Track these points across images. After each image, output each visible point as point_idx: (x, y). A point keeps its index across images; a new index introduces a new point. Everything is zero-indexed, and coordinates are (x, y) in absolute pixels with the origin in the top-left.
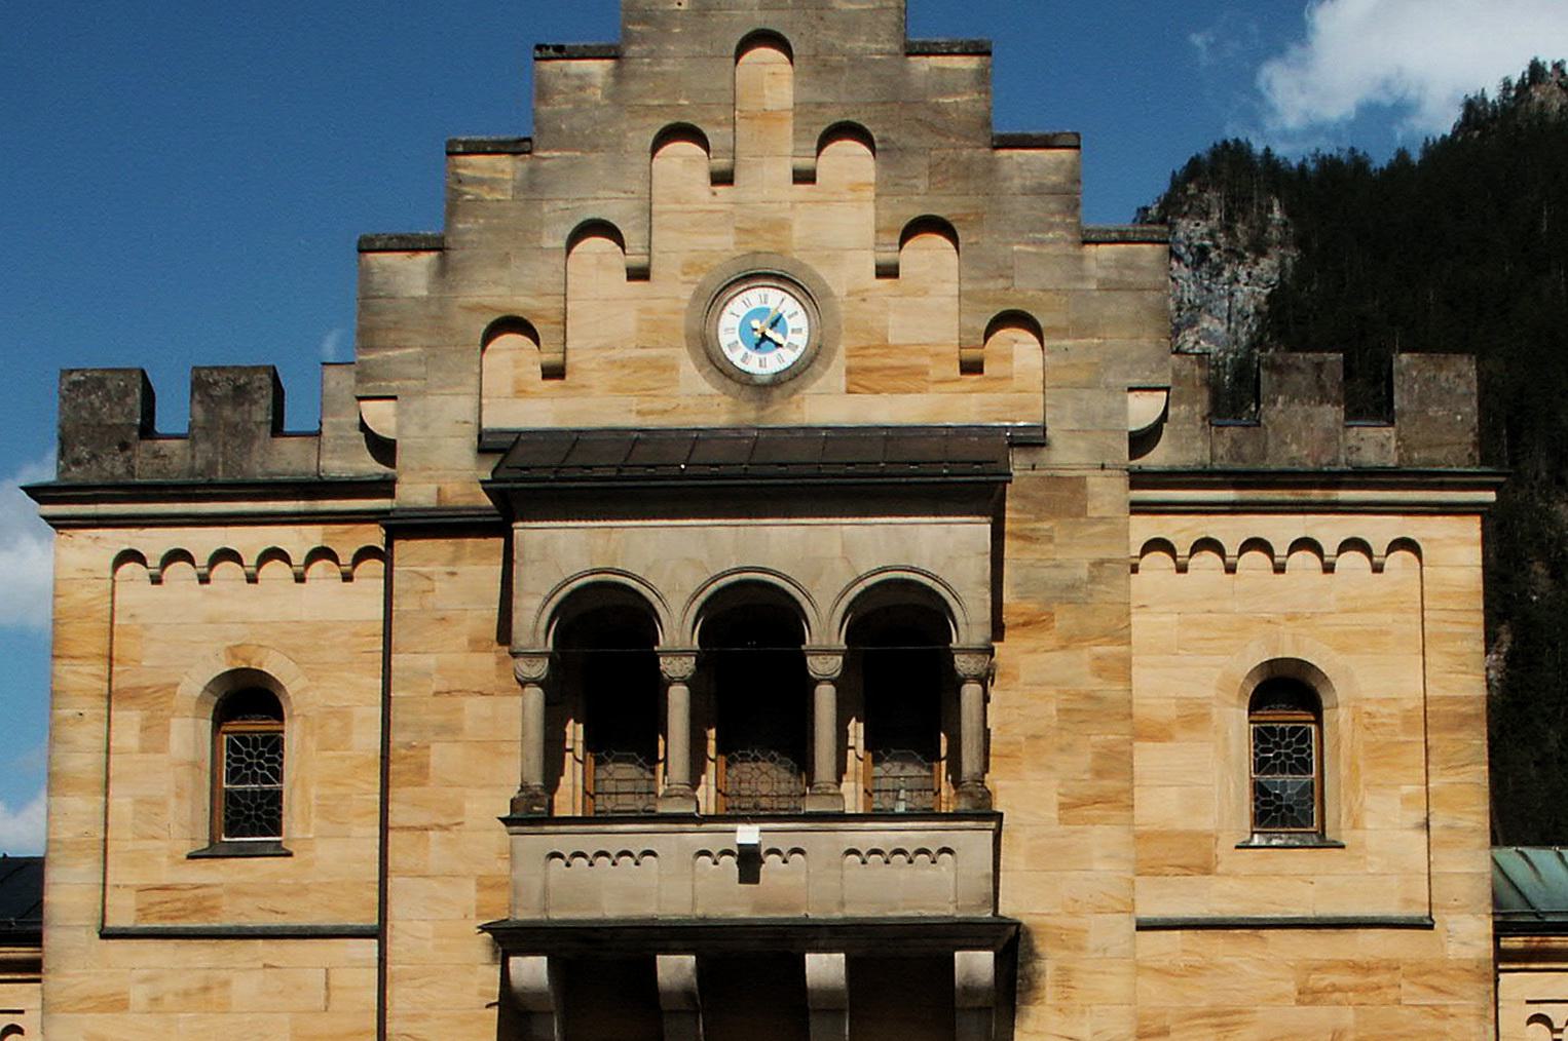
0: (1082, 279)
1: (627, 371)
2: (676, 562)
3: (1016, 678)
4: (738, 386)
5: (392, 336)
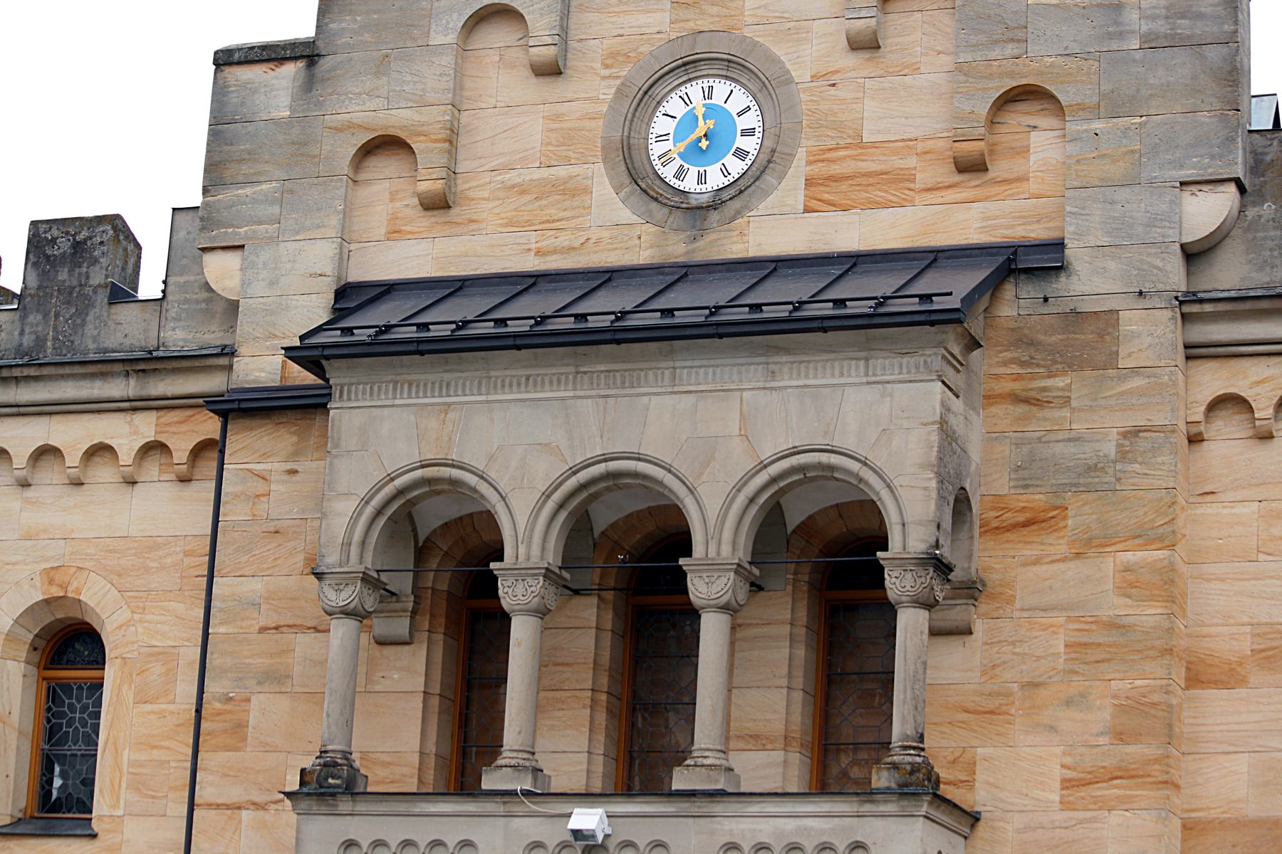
1: (528, 198)
2: (523, 448)
3: (1011, 600)
4: (666, 210)
5: (245, 169)
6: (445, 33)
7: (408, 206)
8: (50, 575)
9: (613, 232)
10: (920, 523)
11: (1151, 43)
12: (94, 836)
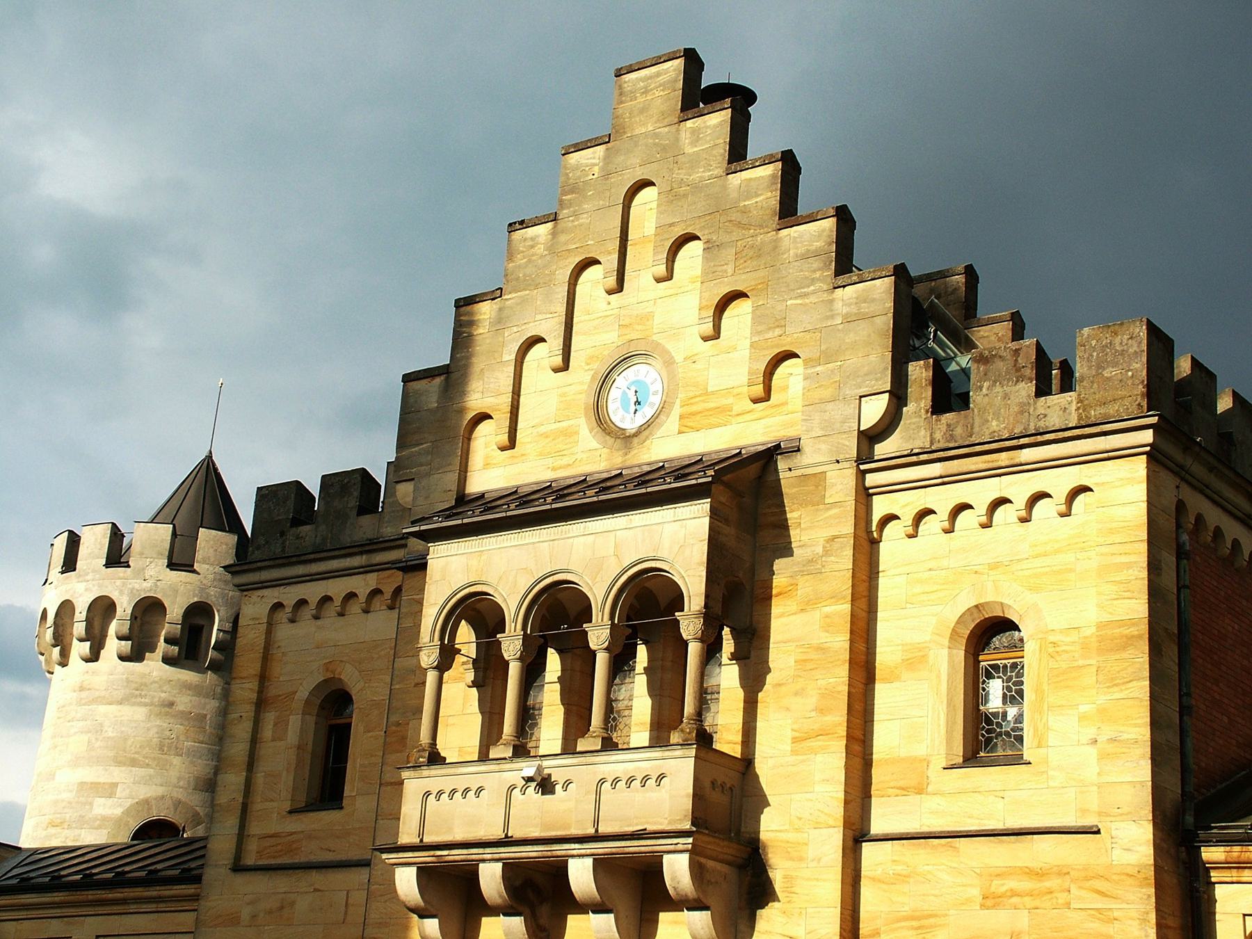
0: (832, 317)
6: (510, 356)
8: (327, 667)
10: (696, 595)
11: (848, 320)
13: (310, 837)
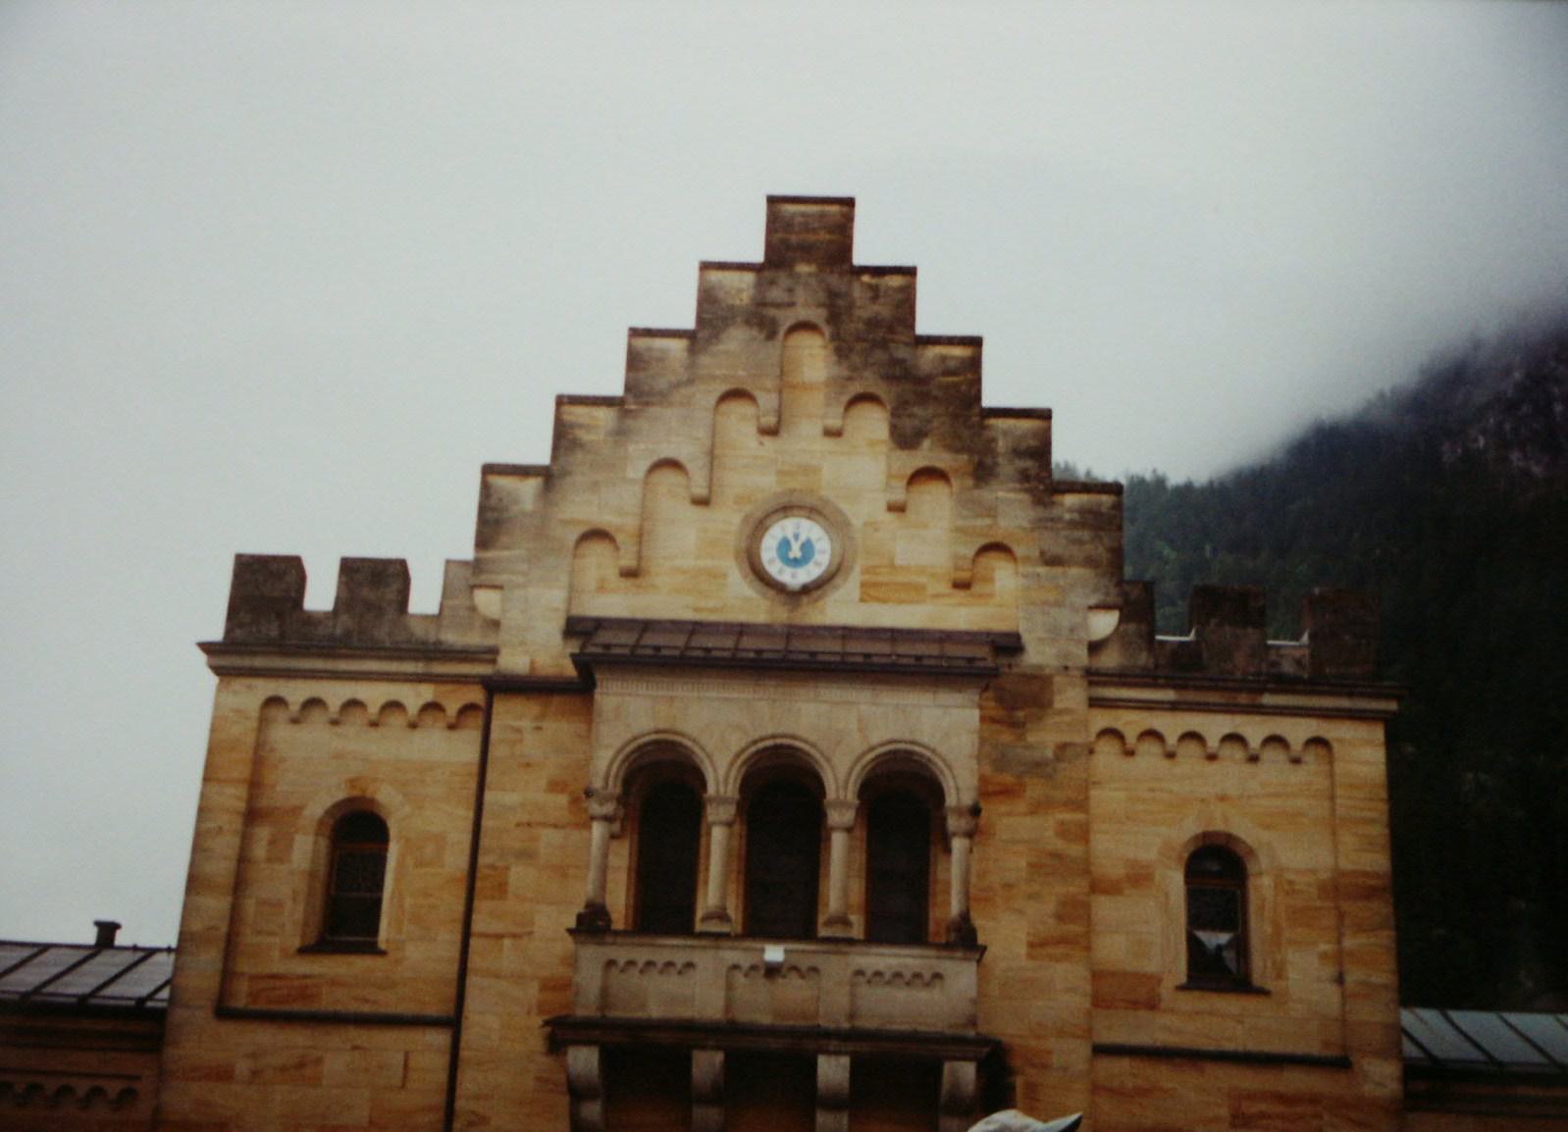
6: (637, 469)
7: (612, 574)
8: (352, 783)
9: (739, 602)
12: (383, 953)
13: (334, 983)
